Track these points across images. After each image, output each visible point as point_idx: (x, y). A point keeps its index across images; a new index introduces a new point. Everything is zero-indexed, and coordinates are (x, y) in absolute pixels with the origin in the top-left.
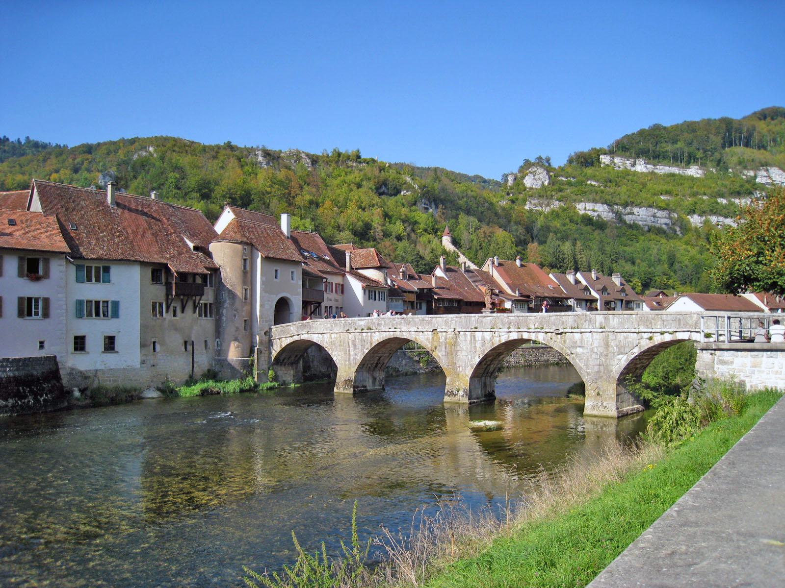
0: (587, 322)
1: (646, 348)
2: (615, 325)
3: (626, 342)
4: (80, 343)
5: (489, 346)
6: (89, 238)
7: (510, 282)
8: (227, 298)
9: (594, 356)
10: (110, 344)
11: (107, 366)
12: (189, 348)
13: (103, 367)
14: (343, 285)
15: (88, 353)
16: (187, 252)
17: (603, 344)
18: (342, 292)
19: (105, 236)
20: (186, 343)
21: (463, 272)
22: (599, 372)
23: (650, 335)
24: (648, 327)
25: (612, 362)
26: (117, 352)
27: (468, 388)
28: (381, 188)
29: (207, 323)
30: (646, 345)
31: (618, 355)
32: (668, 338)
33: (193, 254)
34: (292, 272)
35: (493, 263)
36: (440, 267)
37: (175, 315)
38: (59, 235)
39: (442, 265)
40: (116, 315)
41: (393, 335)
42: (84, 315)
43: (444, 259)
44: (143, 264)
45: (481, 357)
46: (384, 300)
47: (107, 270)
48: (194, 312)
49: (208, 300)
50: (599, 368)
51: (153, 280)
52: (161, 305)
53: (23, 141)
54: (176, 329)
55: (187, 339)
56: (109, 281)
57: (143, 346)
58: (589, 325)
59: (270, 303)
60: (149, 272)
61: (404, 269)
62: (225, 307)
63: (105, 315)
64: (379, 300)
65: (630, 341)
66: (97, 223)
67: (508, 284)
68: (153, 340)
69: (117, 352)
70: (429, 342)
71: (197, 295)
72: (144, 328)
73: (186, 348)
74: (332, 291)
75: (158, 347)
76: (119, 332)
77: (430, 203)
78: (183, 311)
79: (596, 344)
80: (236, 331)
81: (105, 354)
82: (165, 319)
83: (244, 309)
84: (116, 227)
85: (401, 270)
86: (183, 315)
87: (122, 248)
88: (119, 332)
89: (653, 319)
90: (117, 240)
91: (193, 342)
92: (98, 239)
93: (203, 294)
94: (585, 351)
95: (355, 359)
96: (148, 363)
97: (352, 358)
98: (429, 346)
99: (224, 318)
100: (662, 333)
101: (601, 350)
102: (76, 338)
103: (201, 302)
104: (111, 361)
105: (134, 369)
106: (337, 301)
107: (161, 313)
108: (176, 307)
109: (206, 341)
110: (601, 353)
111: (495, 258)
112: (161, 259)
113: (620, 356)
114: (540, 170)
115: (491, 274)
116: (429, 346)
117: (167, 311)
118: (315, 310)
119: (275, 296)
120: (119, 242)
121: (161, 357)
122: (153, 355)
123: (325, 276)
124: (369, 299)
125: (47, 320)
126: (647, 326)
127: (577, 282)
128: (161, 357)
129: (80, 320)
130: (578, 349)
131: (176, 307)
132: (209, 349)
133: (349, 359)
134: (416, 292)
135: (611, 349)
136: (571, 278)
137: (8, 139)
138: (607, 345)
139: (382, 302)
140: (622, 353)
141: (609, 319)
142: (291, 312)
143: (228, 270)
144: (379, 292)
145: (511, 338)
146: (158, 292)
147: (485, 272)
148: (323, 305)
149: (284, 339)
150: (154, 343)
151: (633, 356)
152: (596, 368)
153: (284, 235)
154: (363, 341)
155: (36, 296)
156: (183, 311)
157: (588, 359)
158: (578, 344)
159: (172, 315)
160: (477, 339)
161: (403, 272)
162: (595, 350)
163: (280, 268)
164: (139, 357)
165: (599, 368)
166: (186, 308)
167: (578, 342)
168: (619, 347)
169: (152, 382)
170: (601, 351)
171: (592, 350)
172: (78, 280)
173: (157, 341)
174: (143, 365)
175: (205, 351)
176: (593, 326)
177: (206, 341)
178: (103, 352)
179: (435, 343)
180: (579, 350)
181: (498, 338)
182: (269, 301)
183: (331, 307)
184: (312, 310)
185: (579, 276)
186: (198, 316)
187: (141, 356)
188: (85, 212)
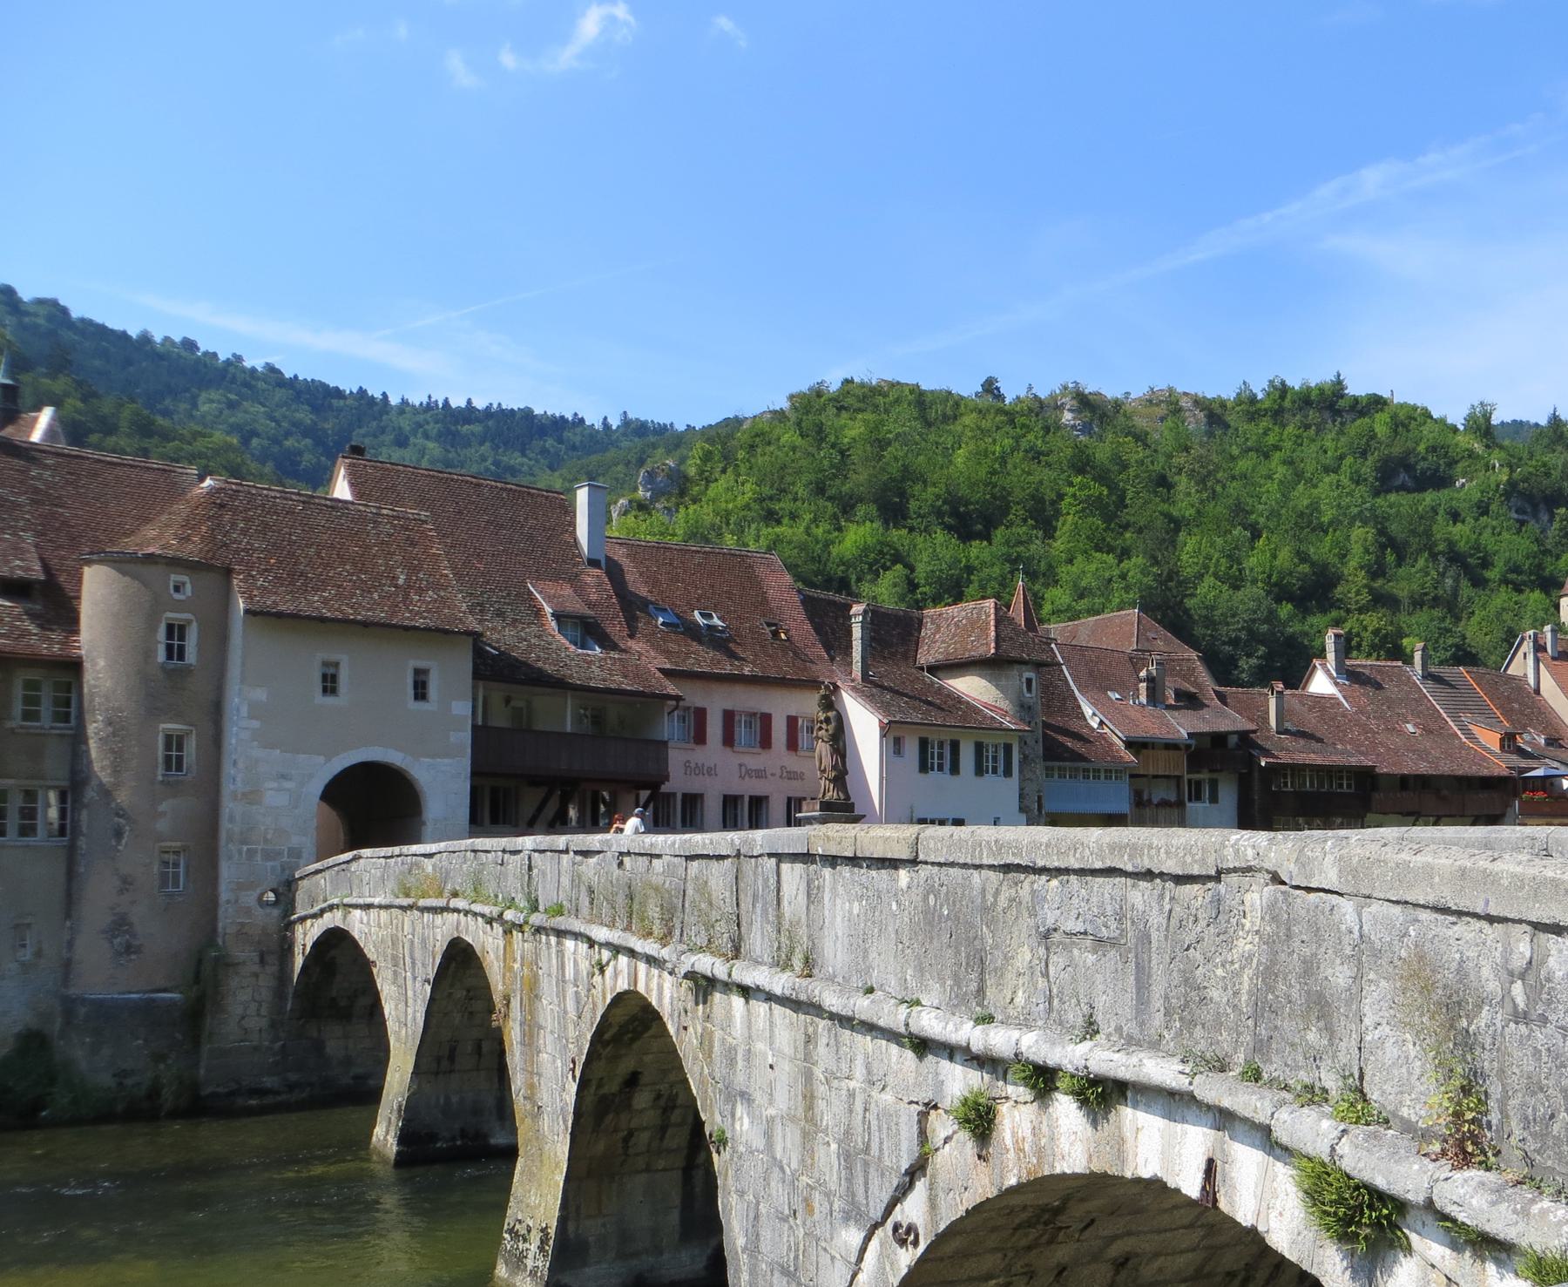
21: (1417, 679)
39: (1331, 656)
43: (1337, 636)
53: (615, 423)
61: (1153, 669)
62: (86, 801)
74: (766, 742)
80: (121, 892)
85: (1143, 674)
99: (82, 843)
115: (1531, 681)
116: (500, 987)
119: (322, 759)
134: (1188, 747)
137: (582, 421)
143: (102, 663)
147: (1513, 678)
153: (580, 556)
160: (567, 978)
161: (1150, 680)
182: (284, 777)
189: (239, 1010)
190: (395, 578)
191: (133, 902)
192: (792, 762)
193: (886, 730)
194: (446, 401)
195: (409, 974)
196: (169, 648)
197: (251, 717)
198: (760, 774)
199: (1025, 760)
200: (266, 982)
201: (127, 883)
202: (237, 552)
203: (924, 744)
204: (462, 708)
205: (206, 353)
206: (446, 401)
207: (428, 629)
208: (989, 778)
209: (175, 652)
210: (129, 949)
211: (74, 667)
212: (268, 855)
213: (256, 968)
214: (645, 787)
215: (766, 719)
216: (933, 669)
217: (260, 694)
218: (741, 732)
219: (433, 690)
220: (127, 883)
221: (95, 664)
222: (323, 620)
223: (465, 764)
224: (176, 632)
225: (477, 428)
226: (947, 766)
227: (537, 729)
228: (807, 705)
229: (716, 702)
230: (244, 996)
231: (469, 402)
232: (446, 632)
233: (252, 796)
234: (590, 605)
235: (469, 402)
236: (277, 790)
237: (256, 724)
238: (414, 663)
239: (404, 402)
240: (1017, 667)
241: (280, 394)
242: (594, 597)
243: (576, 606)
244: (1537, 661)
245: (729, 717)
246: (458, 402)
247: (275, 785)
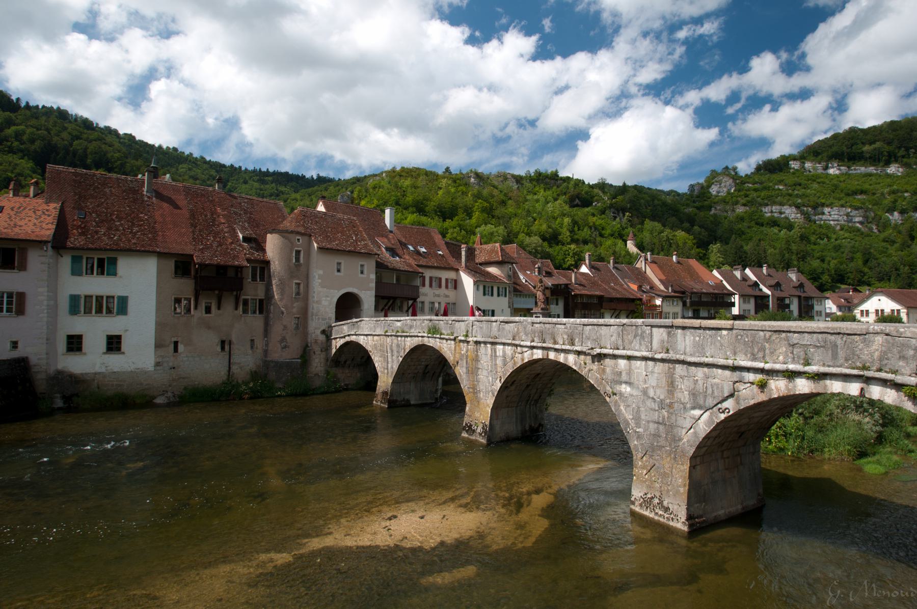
0: (638, 338)
1: (752, 402)
2: (688, 350)
3: (709, 387)
4: (75, 343)
5: (511, 366)
7: (663, 278)
9: (650, 403)
10: (114, 344)
11: (108, 368)
12: (227, 347)
13: (103, 370)
14: (456, 281)
15: (85, 354)
17: (664, 381)
18: (455, 288)
20: (223, 342)
22: (656, 436)
23: (759, 377)
24: (754, 359)
25: (680, 421)
26: (123, 353)
27: (488, 423)
28: (575, 200)
29: (255, 321)
30: (750, 395)
31: (694, 408)
32: (803, 386)
33: (240, 245)
34: (362, 266)
35: (646, 259)
36: (585, 264)
37: (208, 310)
41: (422, 341)
45: (503, 381)
46: (506, 296)
47: (113, 262)
48: (236, 309)
50: (658, 428)
51: (176, 273)
53: (315, 177)
54: (209, 328)
55: (224, 338)
56: (115, 274)
57: (158, 345)
58: (640, 344)
59: (328, 299)
60: (171, 264)
63: (109, 311)
64: (498, 295)
65: (717, 385)
66: (117, 211)
67: (660, 280)
68: (175, 339)
69: (123, 353)
70: (452, 353)
72: (161, 326)
73: (223, 348)
74: (440, 286)
75: (181, 348)
77: (618, 212)
78: (219, 308)
79: (653, 381)
80: (283, 330)
81: (107, 356)
82: (193, 316)
83: (295, 305)
88: (127, 330)
89: (768, 340)
90: (135, 229)
94: (635, 393)
95: (392, 368)
96: (165, 365)
97: (390, 365)
98: (452, 358)
99: (271, 315)
100: (791, 375)
101: (661, 394)
102: (70, 337)
104: (115, 363)
105: (146, 373)
106: (447, 296)
107: (189, 310)
109: (252, 341)
110: (661, 400)
111: (649, 253)
113: (697, 412)
114: (726, 179)
116: (452, 358)
117: (196, 308)
119: (336, 291)
121: (185, 359)
122: (174, 356)
123: (420, 270)
124: (484, 294)
125: (21, 317)
126: (753, 354)
127: (745, 279)
128: (185, 359)
129: (75, 317)
130: (624, 386)
132: (257, 348)
133: (388, 366)
135: (678, 395)
136: (738, 274)
137: (305, 176)
138: (671, 385)
139: (500, 298)
140: (700, 408)
141: (675, 335)
142: (362, 308)
144: (498, 288)
145: (535, 357)
146: (186, 286)
149: (338, 339)
150: (176, 344)
151: (723, 416)
152: (652, 426)
154: (398, 346)
155: (10, 289)
156: (219, 308)
157: (639, 408)
158: (624, 377)
159: (204, 312)
160: (498, 354)
162: (651, 393)
163: (344, 261)
164: (153, 359)
165: (658, 428)
167: (624, 374)
168: (694, 394)
169: (170, 386)
170: (662, 397)
171: (645, 392)
173: (179, 339)
174: (158, 368)
175: (250, 351)
176: (647, 347)
177: (252, 341)
178: (104, 353)
179: (457, 355)
180: (625, 389)
181: (520, 355)
182: (328, 297)
185: (748, 271)
186: (241, 313)
187: (156, 358)
189: (316, 365)
190: (352, 238)
191: (287, 333)
192: (447, 292)
193: (475, 283)
194: (260, 169)
195: (389, 354)
196: (296, 258)
197: (319, 279)
198: (438, 296)
199: (509, 292)
200: (323, 355)
201: (285, 327)
202: (311, 230)
203: (484, 287)
204: (373, 276)
205: (181, 152)
206: (260, 169)
207: (365, 253)
208: (487, 296)
209: (298, 259)
210: (285, 347)
211: (267, 263)
212: (324, 319)
213: (320, 353)
214: (411, 299)
215: (440, 279)
216: (481, 264)
217: (321, 272)
218: (434, 284)
219: (365, 271)
220: (285, 327)
221: (274, 263)
222: (338, 250)
223: (373, 293)
224: (298, 252)
225: (270, 178)
226: (490, 294)
227: (383, 281)
228: (451, 275)
229: (428, 274)
230: (317, 360)
231: (268, 169)
232: (370, 254)
233: (319, 302)
234: (393, 245)
235: (268, 169)
236: (325, 300)
237: (320, 281)
238: (361, 263)
239: (246, 169)
240: (507, 264)
241: (205, 166)
242: (393, 242)
243: (390, 246)
244: (645, 263)
245: (431, 278)
246: (264, 169)
247: (324, 299)
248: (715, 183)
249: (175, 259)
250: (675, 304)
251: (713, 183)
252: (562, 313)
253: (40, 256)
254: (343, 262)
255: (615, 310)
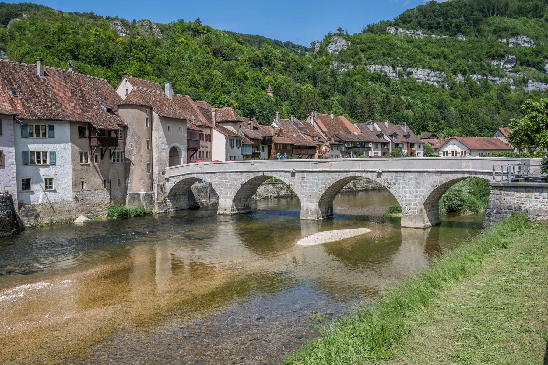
6: (28, 103)
8: (135, 148)
10: (49, 183)
16: (103, 113)
19: (40, 101)
38: (6, 101)
40: (53, 163)
42: (28, 162)
44: (72, 123)
48: (110, 158)
49: (119, 149)
51: (80, 135)
52: (86, 153)
57: (75, 185)
68: (82, 180)
71: (113, 146)
76: (56, 175)
78: (102, 158)
84: (47, 94)
86: (102, 161)
87: (54, 111)
90: (50, 104)
91: (110, 181)
92: (35, 104)
93: (117, 145)
103: (116, 151)
108: (97, 155)
109: (119, 180)
112: (84, 118)
114: (341, 39)
118: (193, 155)
120: (52, 106)
123: (200, 129)
129: (26, 167)
131: (97, 155)
142: (180, 156)
148: (199, 150)
150: (82, 182)
163: (171, 125)
166: (105, 156)
172: (23, 137)
173: (84, 180)
183: (203, 152)
184: (191, 155)
188: (22, 82)
248: (332, 43)
249: (78, 125)
250: (334, 149)
251: (330, 43)
252: (267, 158)
253: (8, 125)
254: (171, 125)
255: (300, 154)
